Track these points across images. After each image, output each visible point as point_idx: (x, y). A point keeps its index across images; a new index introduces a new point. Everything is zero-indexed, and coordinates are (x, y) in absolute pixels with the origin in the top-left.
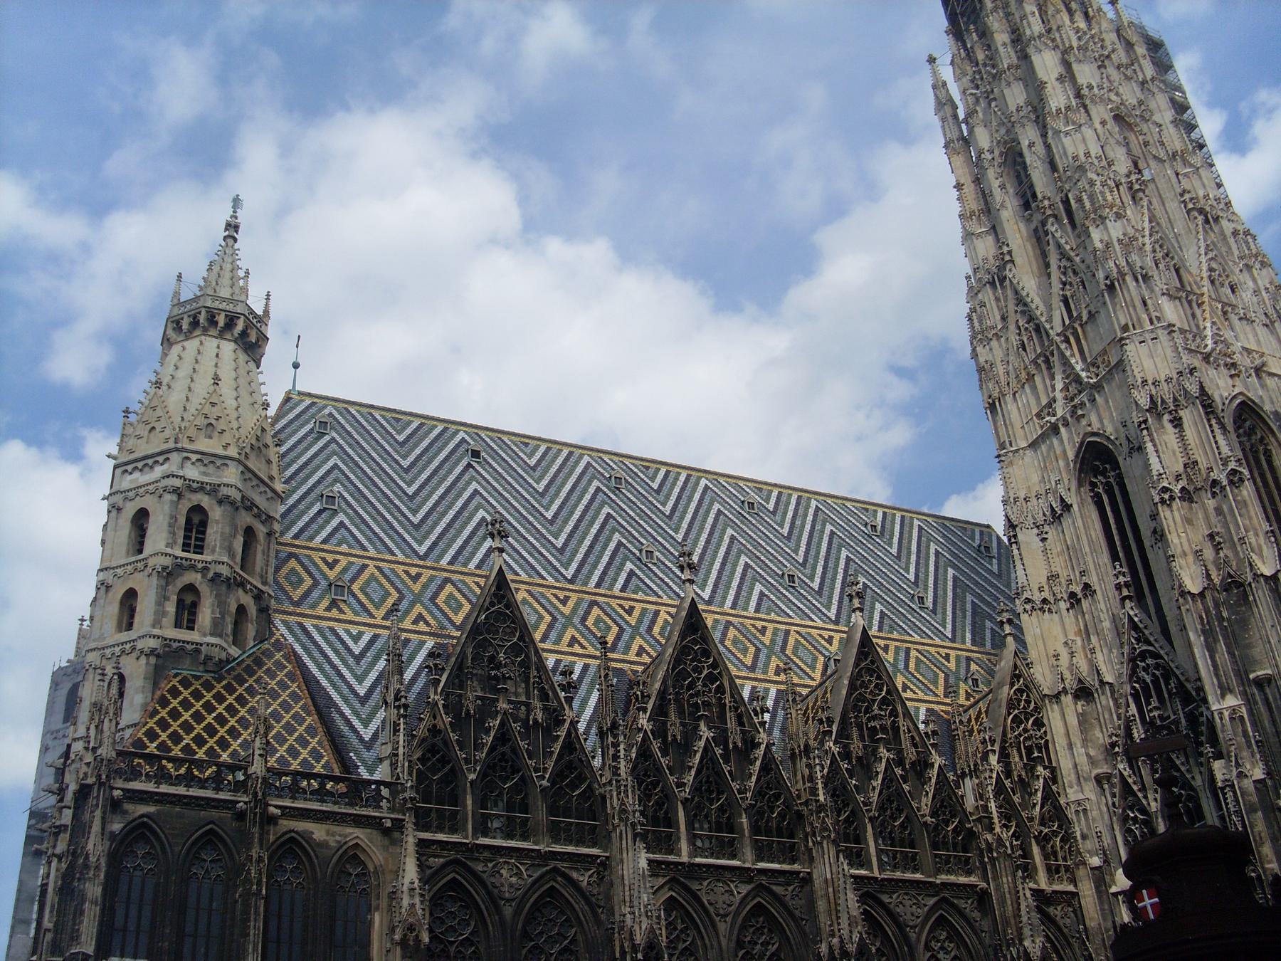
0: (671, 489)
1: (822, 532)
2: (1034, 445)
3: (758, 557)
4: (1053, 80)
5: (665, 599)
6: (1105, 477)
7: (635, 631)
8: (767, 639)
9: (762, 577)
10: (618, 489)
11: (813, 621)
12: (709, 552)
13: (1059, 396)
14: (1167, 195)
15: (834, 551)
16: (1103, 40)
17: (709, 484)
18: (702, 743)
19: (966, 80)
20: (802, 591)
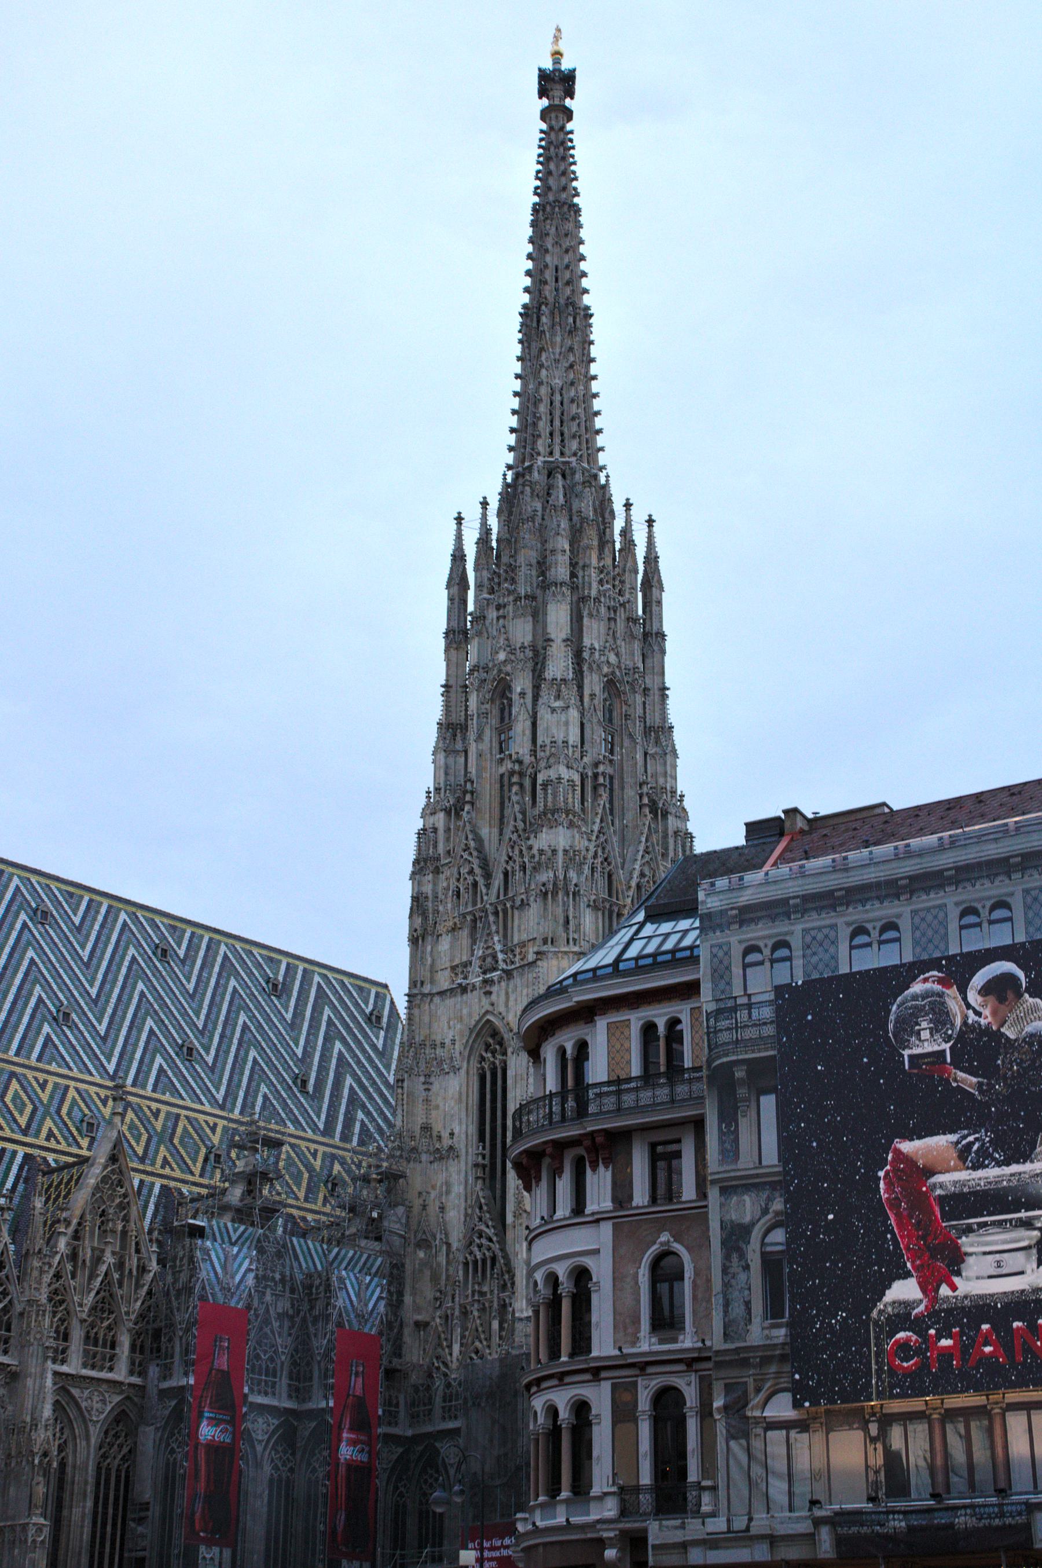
0: (92, 926)
1: (226, 989)
2: (441, 993)
3: (163, 1022)
4: (559, 640)
5: (75, 1073)
6: (494, 1057)
7: (47, 1113)
8: (159, 1125)
9: (163, 1045)
10: (43, 924)
11: (202, 1104)
12: (119, 1013)
13: (476, 963)
14: (628, 780)
15: (232, 1015)
16: (622, 582)
17: (128, 920)
18: (103, 1268)
19: (486, 574)
20: (197, 1067)
